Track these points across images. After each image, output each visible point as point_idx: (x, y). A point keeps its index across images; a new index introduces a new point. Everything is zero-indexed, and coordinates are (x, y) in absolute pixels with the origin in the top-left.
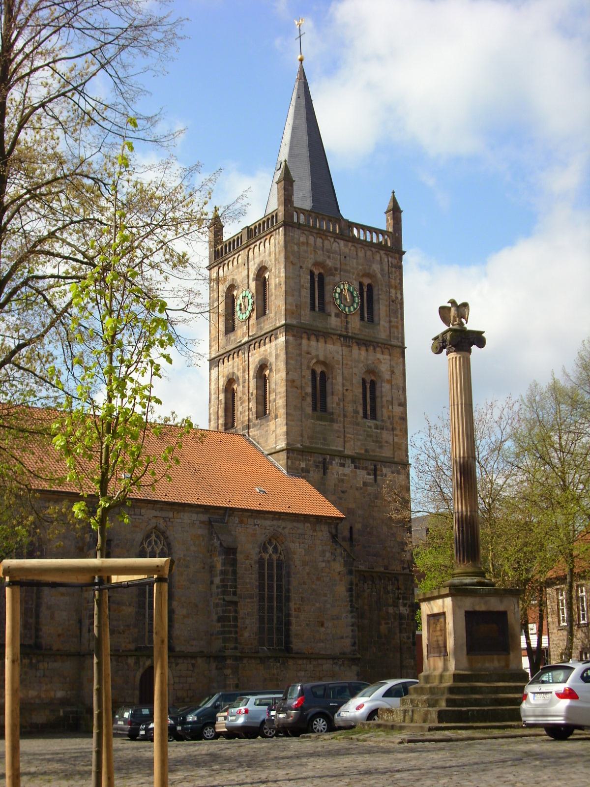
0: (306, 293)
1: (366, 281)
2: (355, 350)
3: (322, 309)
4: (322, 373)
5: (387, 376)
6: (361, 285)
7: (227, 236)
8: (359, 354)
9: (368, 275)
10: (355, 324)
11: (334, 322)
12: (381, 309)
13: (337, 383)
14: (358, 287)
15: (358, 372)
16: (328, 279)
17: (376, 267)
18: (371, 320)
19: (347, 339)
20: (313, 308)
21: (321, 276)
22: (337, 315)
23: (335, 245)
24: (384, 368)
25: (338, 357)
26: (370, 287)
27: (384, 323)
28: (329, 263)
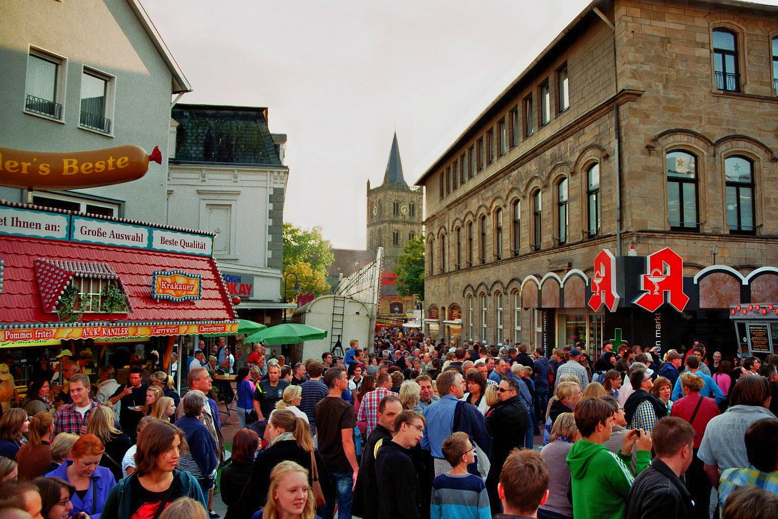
0: (392, 210)
1: (412, 204)
2: (407, 225)
3: (397, 214)
4: (397, 233)
5: (417, 232)
6: (410, 205)
7: (372, 187)
8: (409, 227)
9: (412, 202)
10: (407, 218)
11: (401, 217)
12: (416, 212)
13: (401, 236)
14: (408, 205)
15: (408, 232)
16: (399, 205)
17: (415, 199)
18: (413, 215)
19: (405, 222)
20: (394, 214)
21: (397, 204)
22: (402, 215)
23: (402, 194)
24: (416, 230)
25: (402, 228)
26: (413, 205)
27: (417, 216)
28: (400, 200)
